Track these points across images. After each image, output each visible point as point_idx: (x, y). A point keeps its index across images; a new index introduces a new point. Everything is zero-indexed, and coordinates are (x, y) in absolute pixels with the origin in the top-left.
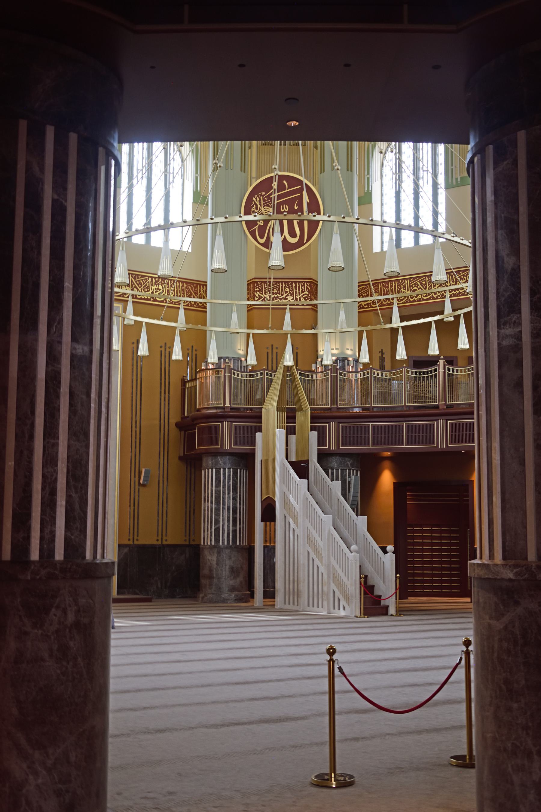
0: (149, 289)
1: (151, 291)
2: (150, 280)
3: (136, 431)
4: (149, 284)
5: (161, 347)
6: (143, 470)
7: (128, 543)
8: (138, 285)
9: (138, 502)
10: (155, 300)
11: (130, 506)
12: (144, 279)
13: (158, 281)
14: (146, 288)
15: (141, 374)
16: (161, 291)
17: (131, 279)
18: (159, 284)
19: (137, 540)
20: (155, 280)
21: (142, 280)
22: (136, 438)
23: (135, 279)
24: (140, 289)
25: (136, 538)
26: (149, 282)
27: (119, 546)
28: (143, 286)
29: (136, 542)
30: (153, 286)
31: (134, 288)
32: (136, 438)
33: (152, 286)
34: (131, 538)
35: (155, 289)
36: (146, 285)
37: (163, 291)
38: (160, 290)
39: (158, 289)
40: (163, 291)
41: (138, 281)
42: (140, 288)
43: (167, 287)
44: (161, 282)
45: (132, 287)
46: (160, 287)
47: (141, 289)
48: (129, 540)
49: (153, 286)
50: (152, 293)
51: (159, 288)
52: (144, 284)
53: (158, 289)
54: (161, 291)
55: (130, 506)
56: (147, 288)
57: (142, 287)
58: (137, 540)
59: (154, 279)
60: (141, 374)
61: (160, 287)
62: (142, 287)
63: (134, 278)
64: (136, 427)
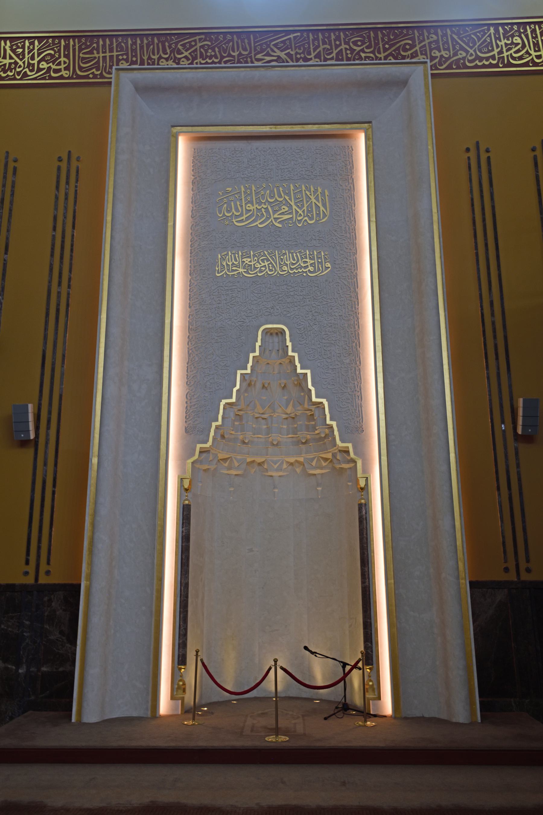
0: (492, 46)
1: (496, 52)
2: (492, 30)
3: (493, 323)
4: (491, 39)
5: (534, 150)
6: (521, 402)
7: (502, 577)
8: (468, 45)
9: (519, 480)
10: (510, 65)
11: (498, 489)
12: (479, 32)
13: (511, 29)
14: (485, 47)
15: (493, 207)
16: (520, 46)
17: (451, 36)
18: (513, 36)
19: (528, 570)
20: (504, 29)
21: (475, 34)
22: (495, 337)
23: (458, 34)
24: (471, 51)
25: (523, 565)
26: (490, 36)
27: (473, 585)
28: (478, 44)
29: (525, 577)
30: (500, 41)
31: (458, 51)
32: (495, 337)
33: (498, 42)
34: (511, 565)
35: (506, 45)
36: (485, 41)
37: (524, 46)
38: (517, 44)
39: (512, 43)
40: (524, 46)
41: (465, 37)
42: (471, 48)
43: (533, 38)
44: (518, 31)
45: (454, 48)
46: (517, 40)
47: (475, 51)
48: (506, 570)
49: (500, 41)
50: (501, 52)
51: (515, 41)
52: (479, 39)
53: (512, 43)
54: (520, 46)
55: (498, 489)
56: (487, 46)
57: (476, 46)
58: (528, 570)
59: (500, 28)
60: (493, 207)
61: (517, 40)
62: (476, 46)
63: (456, 35)
64: (493, 315)
